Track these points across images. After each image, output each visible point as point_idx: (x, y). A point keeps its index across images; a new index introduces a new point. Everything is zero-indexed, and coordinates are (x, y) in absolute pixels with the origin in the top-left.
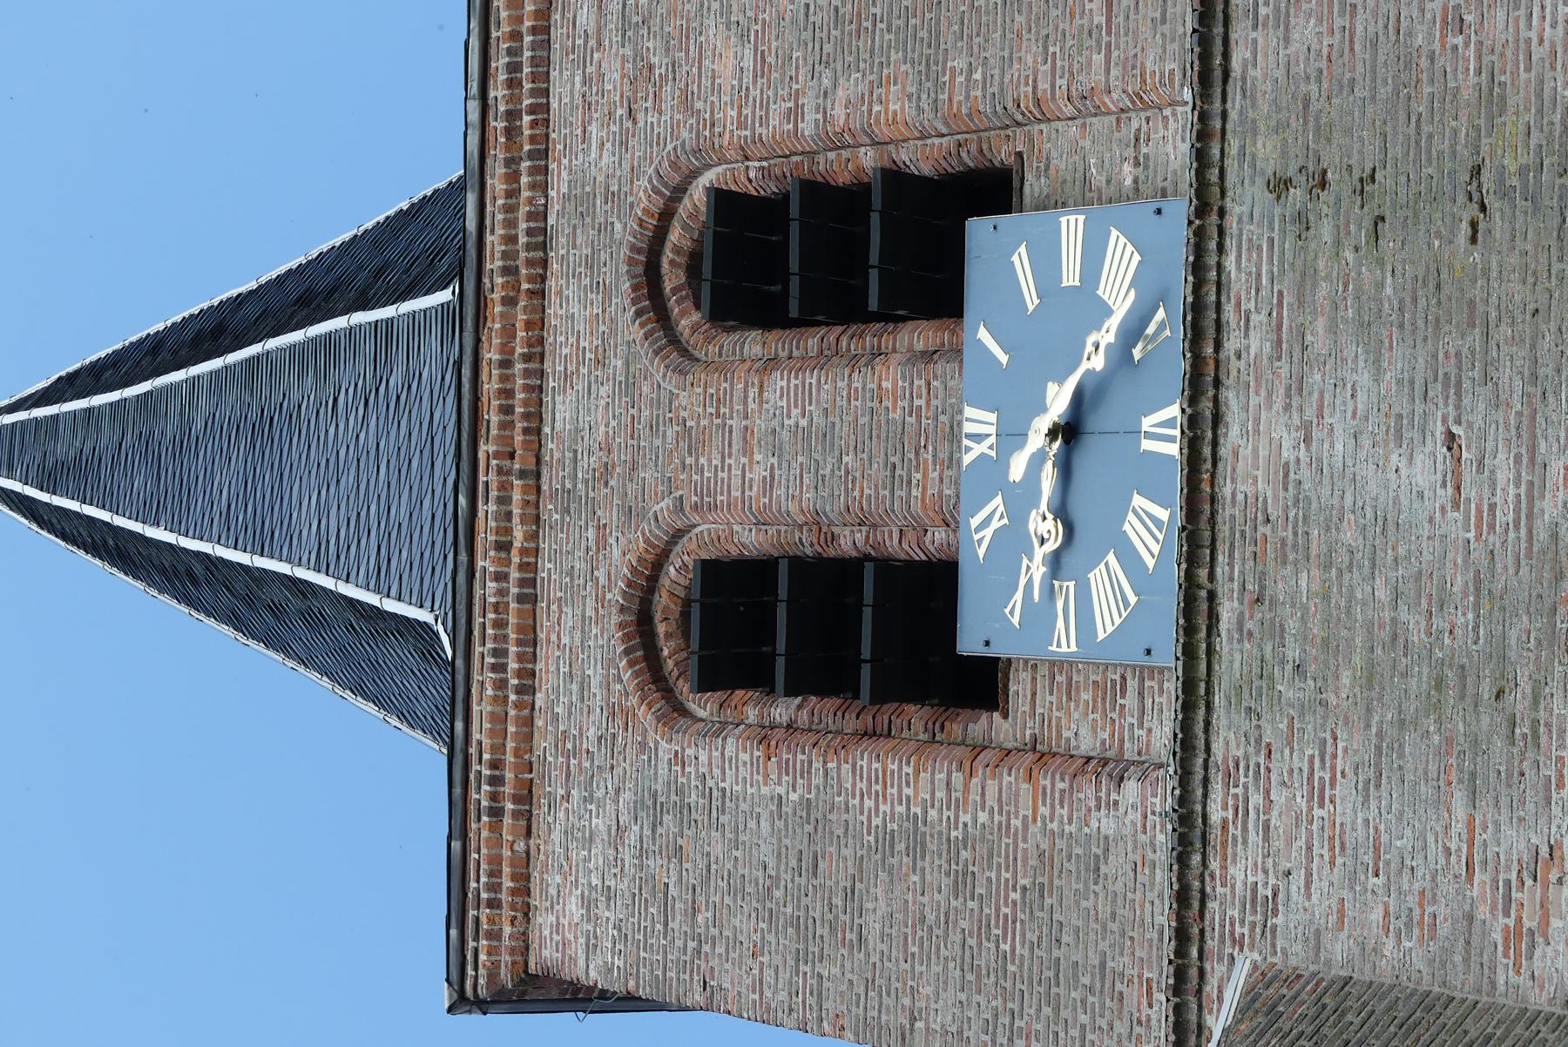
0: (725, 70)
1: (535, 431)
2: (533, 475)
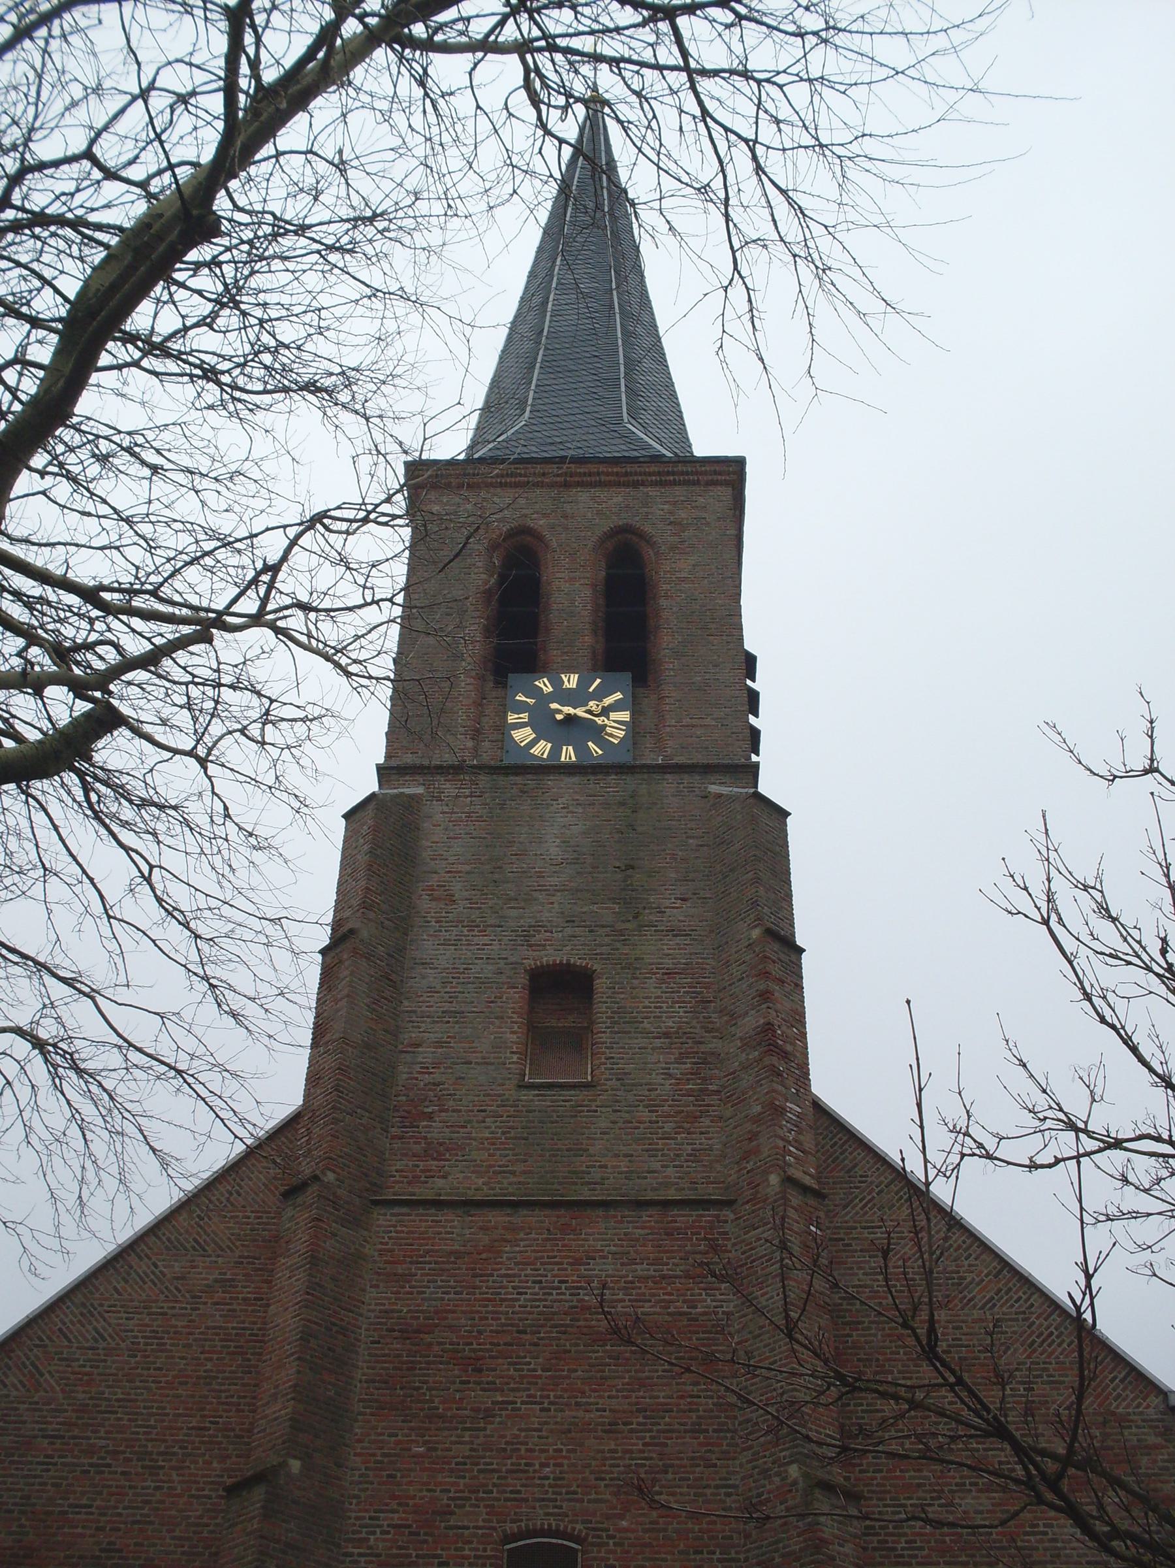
1: (578, 484)
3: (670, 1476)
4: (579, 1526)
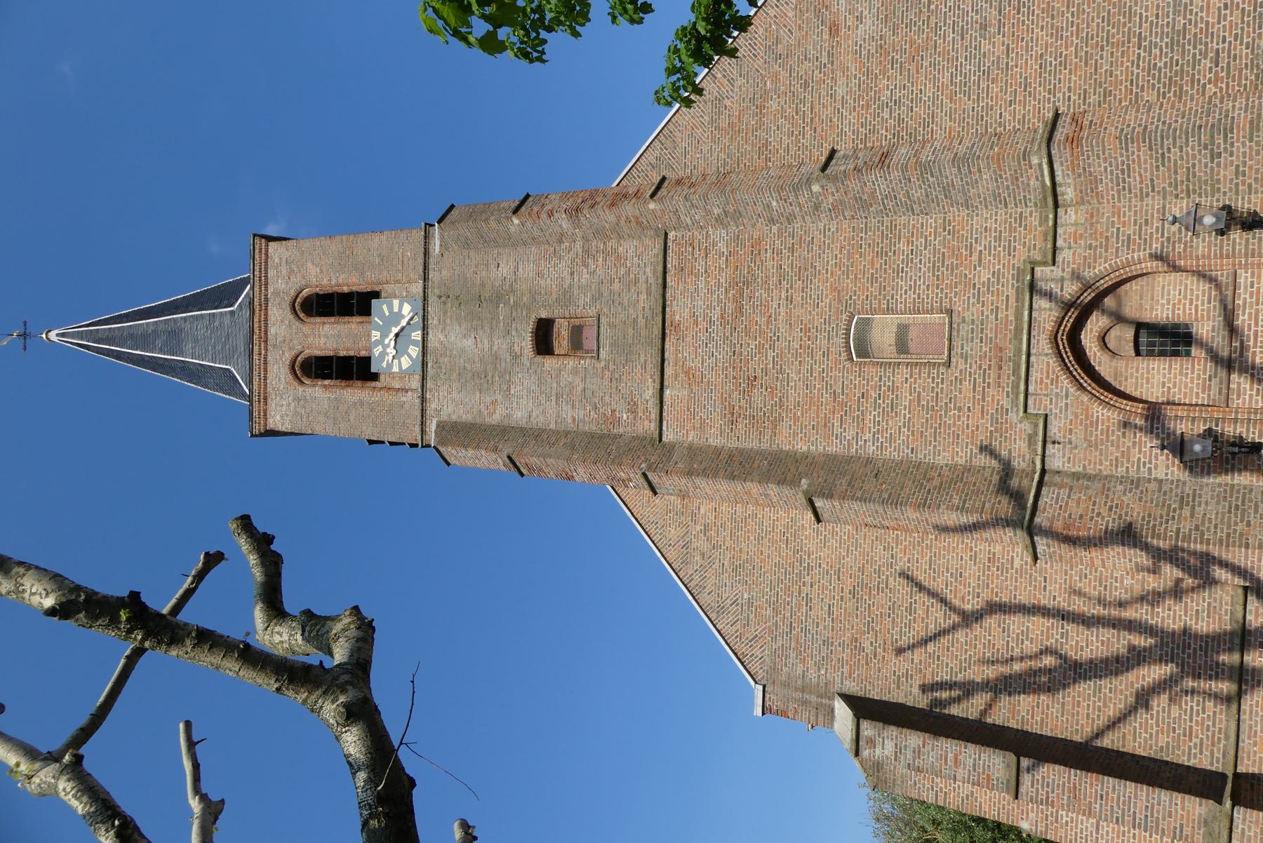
0: (313, 273)
1: (266, 334)
2: (266, 342)
4: (844, 317)
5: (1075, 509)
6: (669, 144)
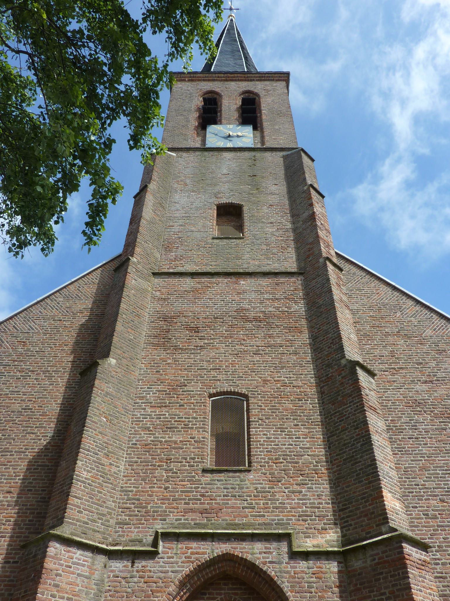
3: (284, 370)
5: (65, 580)
6: (364, 280)
